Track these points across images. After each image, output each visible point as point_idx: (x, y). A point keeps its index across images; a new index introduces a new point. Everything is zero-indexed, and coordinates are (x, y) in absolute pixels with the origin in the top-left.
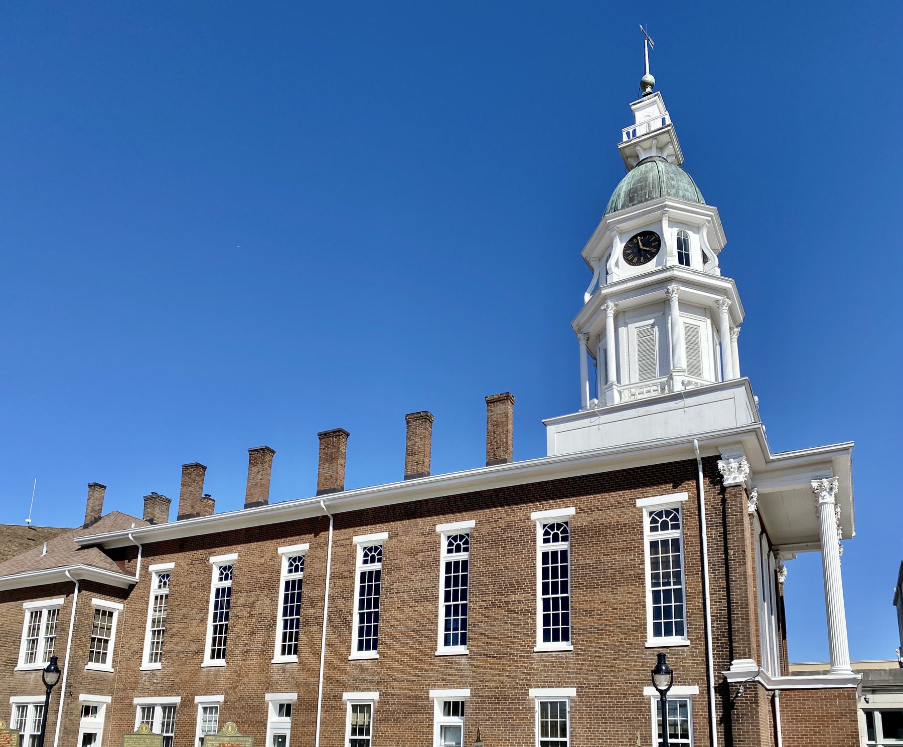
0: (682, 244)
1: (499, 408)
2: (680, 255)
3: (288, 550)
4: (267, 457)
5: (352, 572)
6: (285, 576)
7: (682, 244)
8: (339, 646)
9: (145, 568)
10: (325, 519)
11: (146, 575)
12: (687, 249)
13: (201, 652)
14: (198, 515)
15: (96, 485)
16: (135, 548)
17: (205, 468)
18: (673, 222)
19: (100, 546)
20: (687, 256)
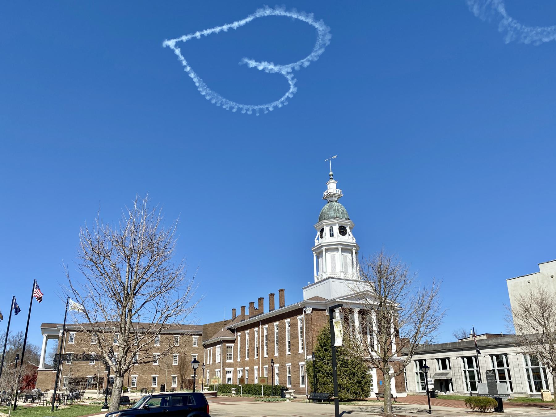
0: (331, 230)
1: (281, 292)
2: (330, 234)
3: (256, 329)
4: (252, 305)
5: (264, 335)
6: (256, 336)
7: (331, 230)
8: (263, 354)
9: (237, 334)
10: (258, 322)
11: (237, 336)
12: (333, 231)
13: (245, 356)
14: (244, 320)
15: (233, 309)
16: (235, 329)
17: (245, 307)
18: (327, 225)
19: (230, 329)
20: (333, 234)
